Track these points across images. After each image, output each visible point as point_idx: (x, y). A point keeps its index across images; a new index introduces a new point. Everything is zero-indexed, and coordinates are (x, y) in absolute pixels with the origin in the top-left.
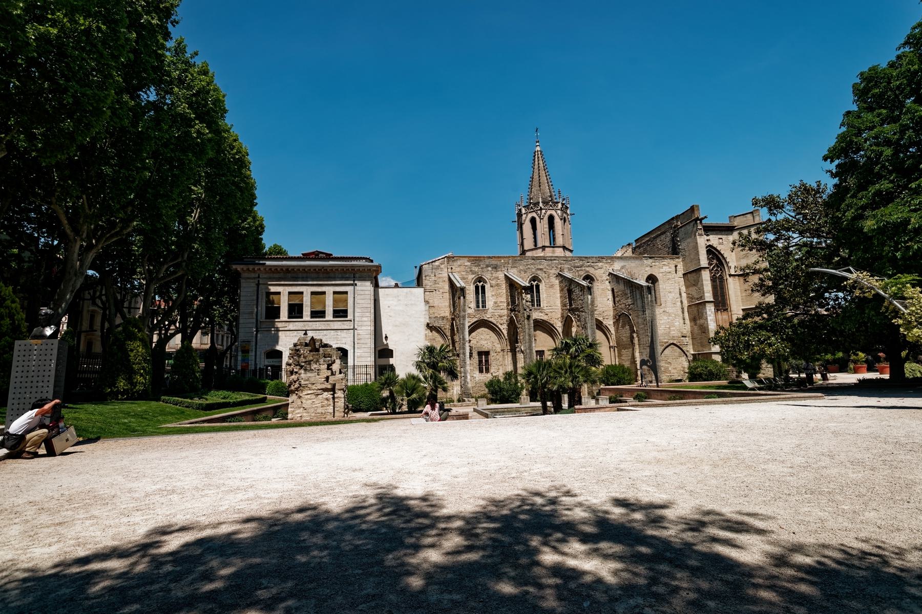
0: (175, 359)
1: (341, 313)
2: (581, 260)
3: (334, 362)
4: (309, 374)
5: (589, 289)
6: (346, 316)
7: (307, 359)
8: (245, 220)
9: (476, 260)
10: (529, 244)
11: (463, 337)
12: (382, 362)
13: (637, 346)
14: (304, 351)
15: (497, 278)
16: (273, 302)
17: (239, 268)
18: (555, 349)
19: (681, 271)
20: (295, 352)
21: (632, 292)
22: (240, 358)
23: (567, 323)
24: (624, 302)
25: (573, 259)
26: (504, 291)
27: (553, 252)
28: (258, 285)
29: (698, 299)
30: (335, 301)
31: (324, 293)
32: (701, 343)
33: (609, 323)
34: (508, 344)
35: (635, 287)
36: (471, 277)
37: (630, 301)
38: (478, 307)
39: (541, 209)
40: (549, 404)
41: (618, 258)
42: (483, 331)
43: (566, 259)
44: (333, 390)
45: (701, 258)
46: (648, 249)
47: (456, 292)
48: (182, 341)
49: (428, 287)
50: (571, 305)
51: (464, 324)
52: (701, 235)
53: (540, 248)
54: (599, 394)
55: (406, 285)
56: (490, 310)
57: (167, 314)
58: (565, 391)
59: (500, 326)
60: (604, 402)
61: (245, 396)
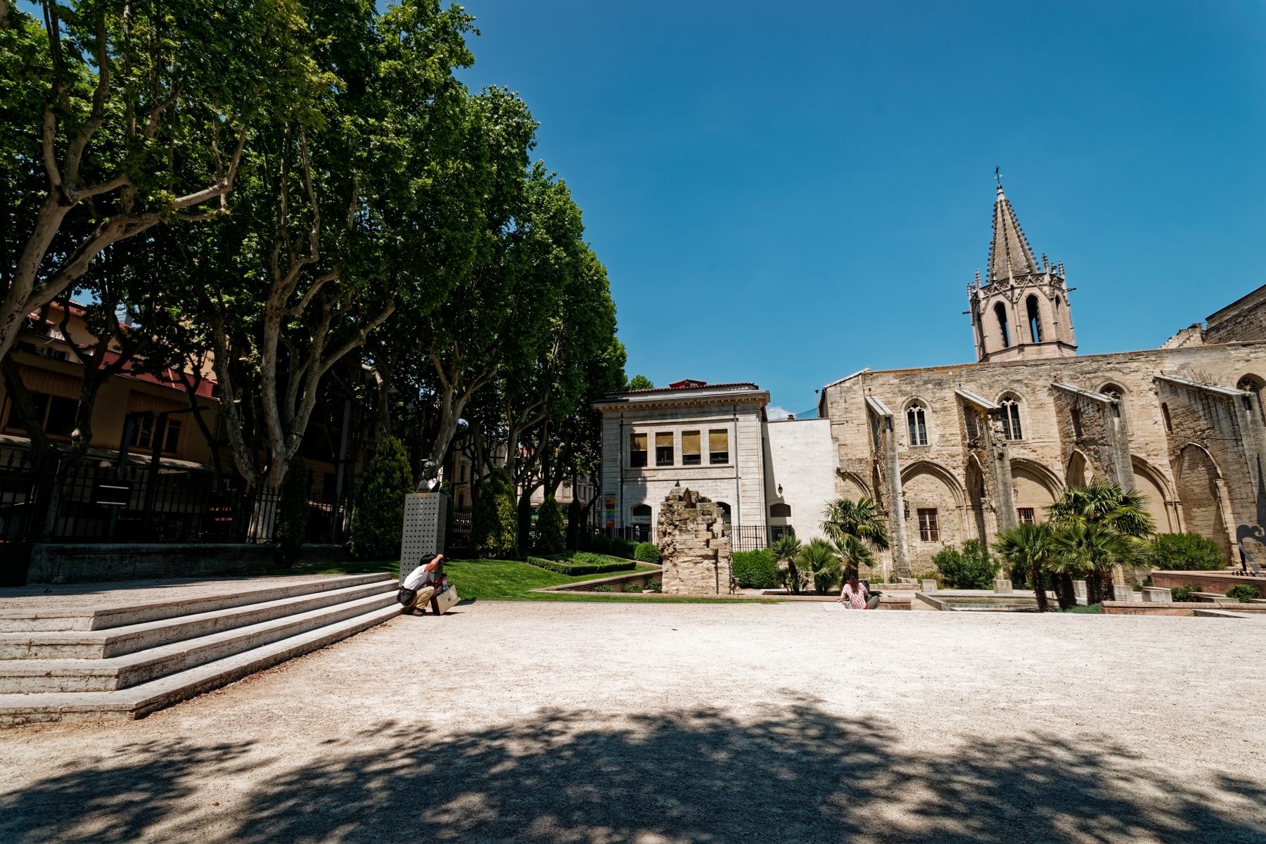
0: (540, 514)
1: (719, 458)
2: (1094, 361)
3: (715, 521)
4: (685, 536)
5: (1115, 407)
6: (727, 462)
7: (682, 517)
8: (604, 350)
9: (907, 375)
10: (994, 341)
11: (893, 487)
12: (777, 521)
13: (1226, 503)
14: (679, 506)
15: (944, 399)
16: (638, 446)
17: (600, 406)
18: (1056, 507)
20: (668, 508)
21: (1207, 408)
22: (604, 514)
23: (1074, 465)
24: (1191, 426)
25: (1078, 360)
26: (957, 418)
27: (1040, 352)
28: (622, 425)
30: (712, 442)
31: (698, 433)
33: (1161, 462)
34: (968, 497)
35: (1214, 399)
36: (901, 400)
37: (1203, 424)
38: (914, 442)
39: (1013, 288)
40: (1049, 594)
41: (1172, 351)
42: (924, 479)
43: (1065, 362)
44: (715, 557)
46: (1239, 329)
47: (878, 423)
48: (546, 494)
49: (836, 418)
50: (1079, 434)
51: (893, 469)
53: (1014, 348)
54: (1148, 581)
55: (804, 417)
56: (935, 448)
57: (530, 462)
58: (1078, 575)
59: (952, 471)
60: (1161, 596)
61: (611, 561)
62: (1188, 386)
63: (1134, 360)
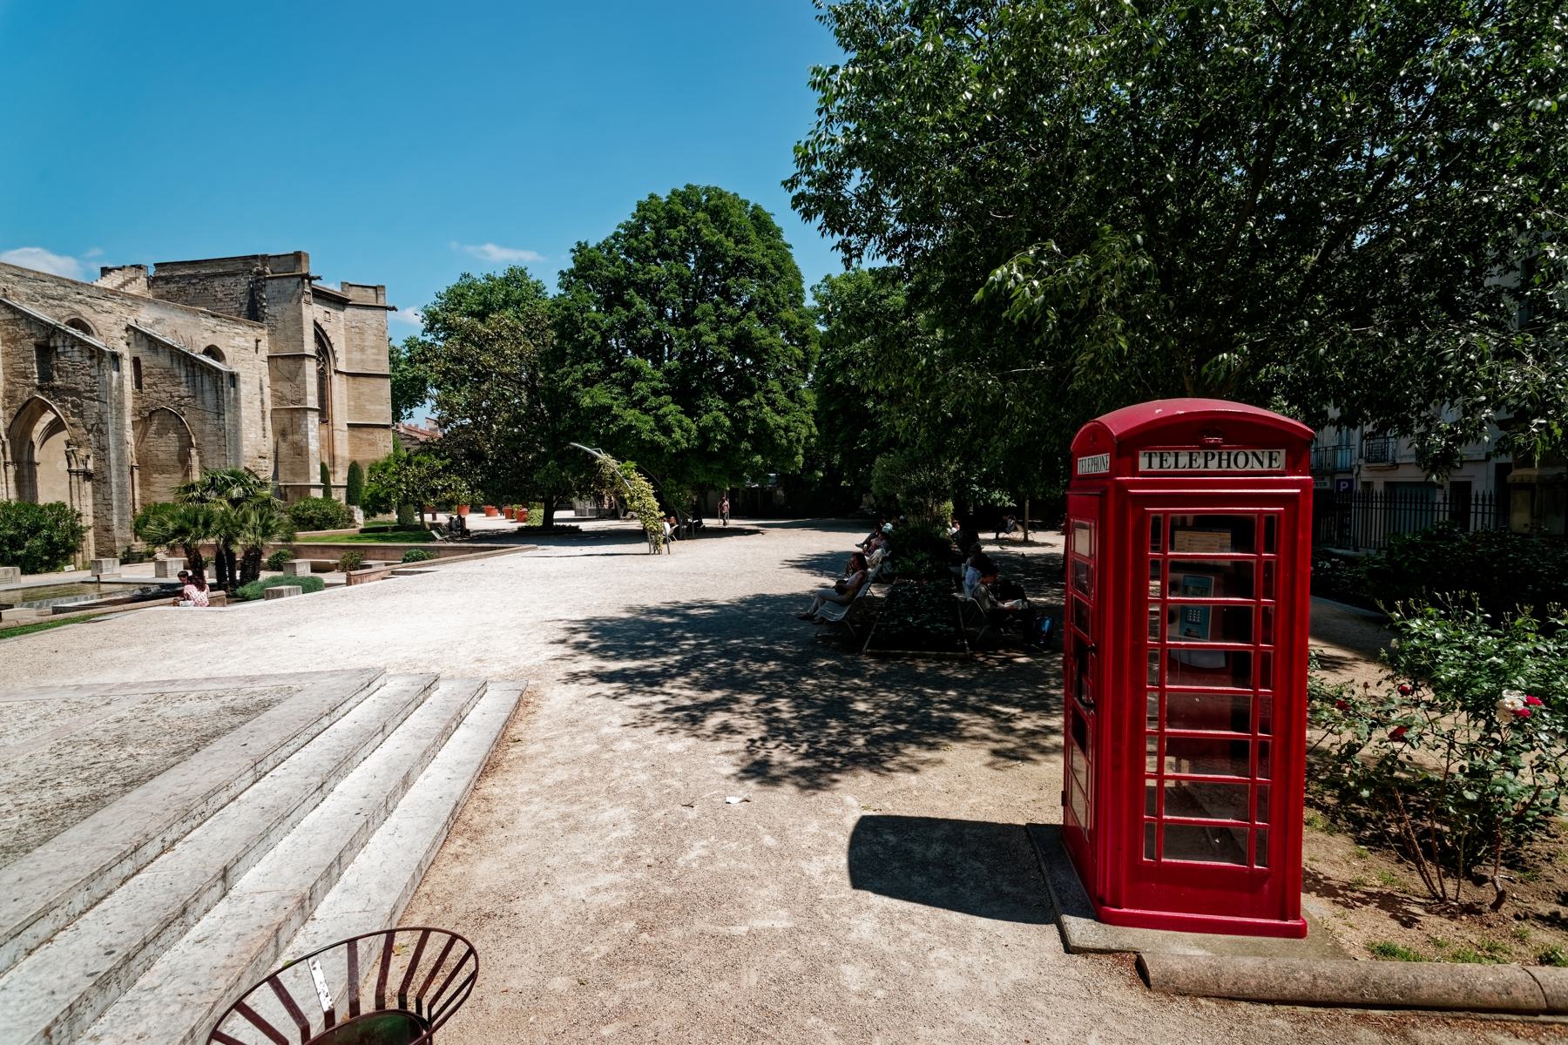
2: (60, 285)
19: (265, 349)
29: (293, 402)
32: (292, 469)
35: (202, 369)
37: (183, 390)
45: (306, 339)
46: (191, 290)
52: (308, 303)
62: (172, 347)
63: (109, 299)
